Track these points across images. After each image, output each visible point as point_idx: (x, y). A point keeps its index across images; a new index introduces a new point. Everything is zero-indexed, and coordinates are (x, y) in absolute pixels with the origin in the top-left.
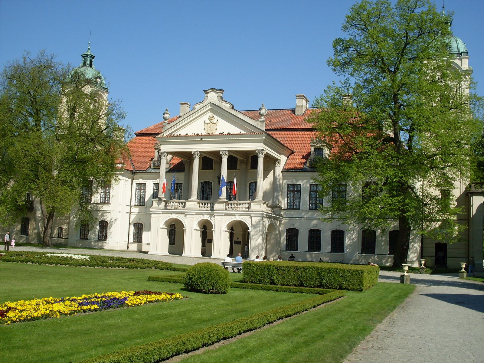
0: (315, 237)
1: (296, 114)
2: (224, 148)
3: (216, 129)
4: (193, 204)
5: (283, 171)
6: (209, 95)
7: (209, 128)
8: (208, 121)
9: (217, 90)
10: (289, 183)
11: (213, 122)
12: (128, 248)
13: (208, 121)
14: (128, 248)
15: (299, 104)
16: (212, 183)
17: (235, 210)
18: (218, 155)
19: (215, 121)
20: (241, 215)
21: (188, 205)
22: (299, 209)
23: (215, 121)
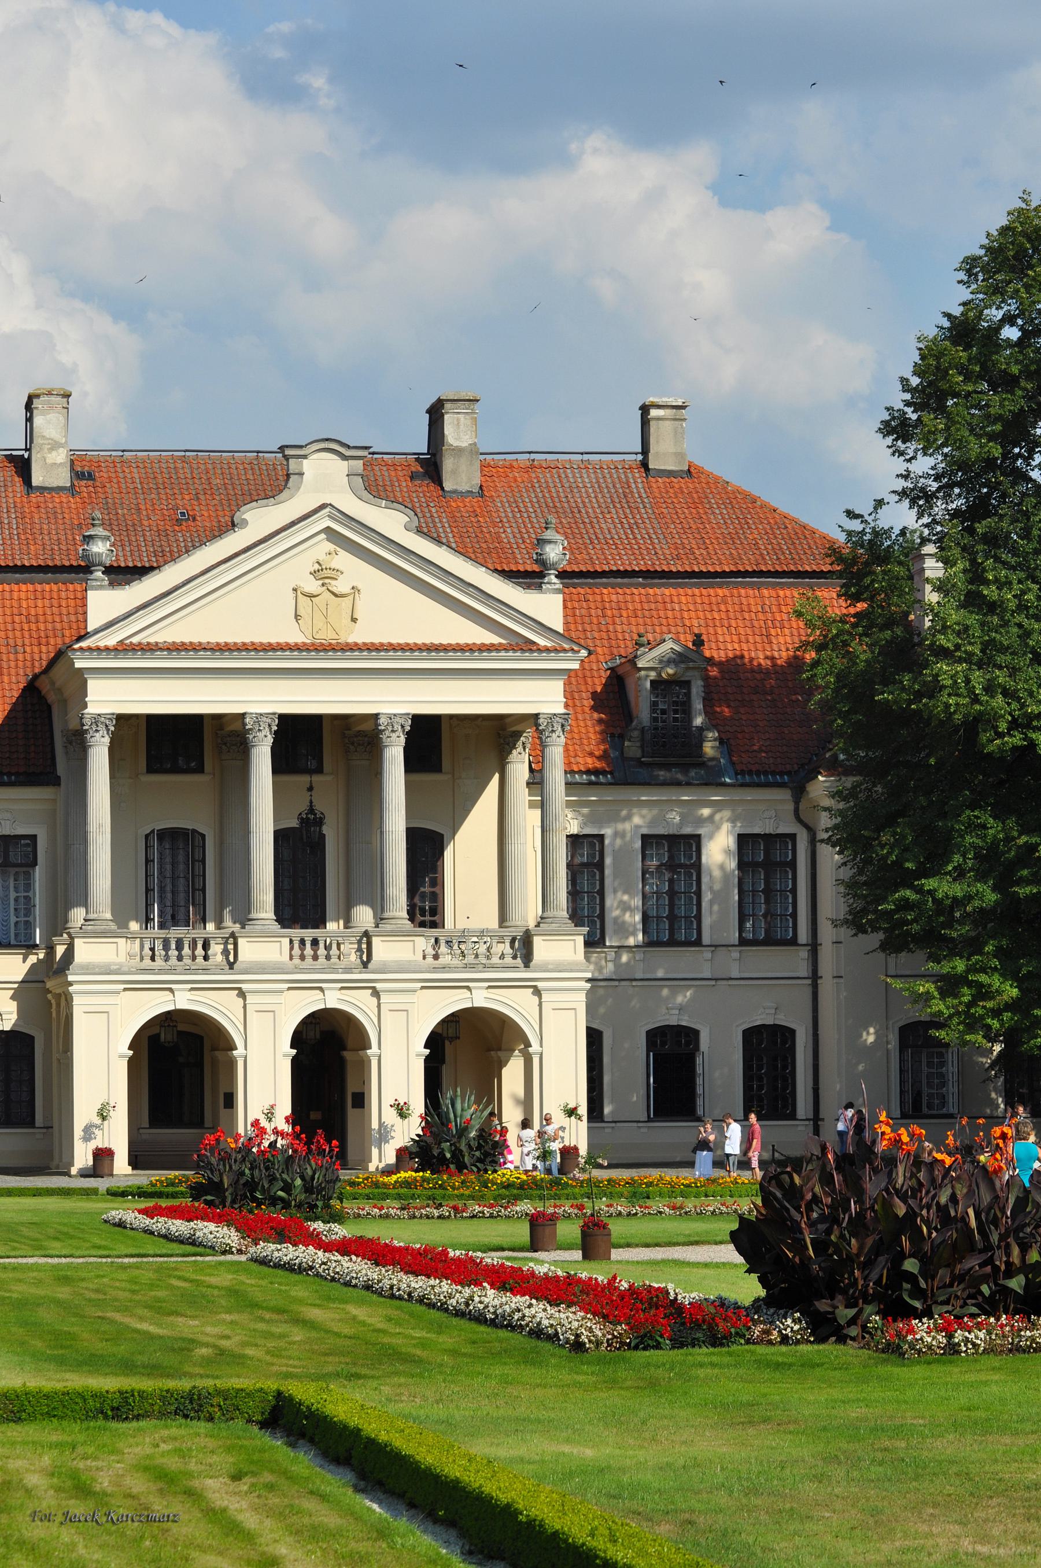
0: (673, 1061)
1: (448, 486)
2: (393, 700)
3: (354, 620)
4: (266, 946)
5: (533, 783)
6: (307, 465)
7: (318, 616)
8: (312, 586)
9: (349, 447)
10: (607, 842)
11: (334, 589)
13: (312, 586)
15: (458, 439)
16: (203, 836)
17: (467, 967)
18: (359, 735)
19: (341, 586)
20: (494, 985)
23: (341, 586)
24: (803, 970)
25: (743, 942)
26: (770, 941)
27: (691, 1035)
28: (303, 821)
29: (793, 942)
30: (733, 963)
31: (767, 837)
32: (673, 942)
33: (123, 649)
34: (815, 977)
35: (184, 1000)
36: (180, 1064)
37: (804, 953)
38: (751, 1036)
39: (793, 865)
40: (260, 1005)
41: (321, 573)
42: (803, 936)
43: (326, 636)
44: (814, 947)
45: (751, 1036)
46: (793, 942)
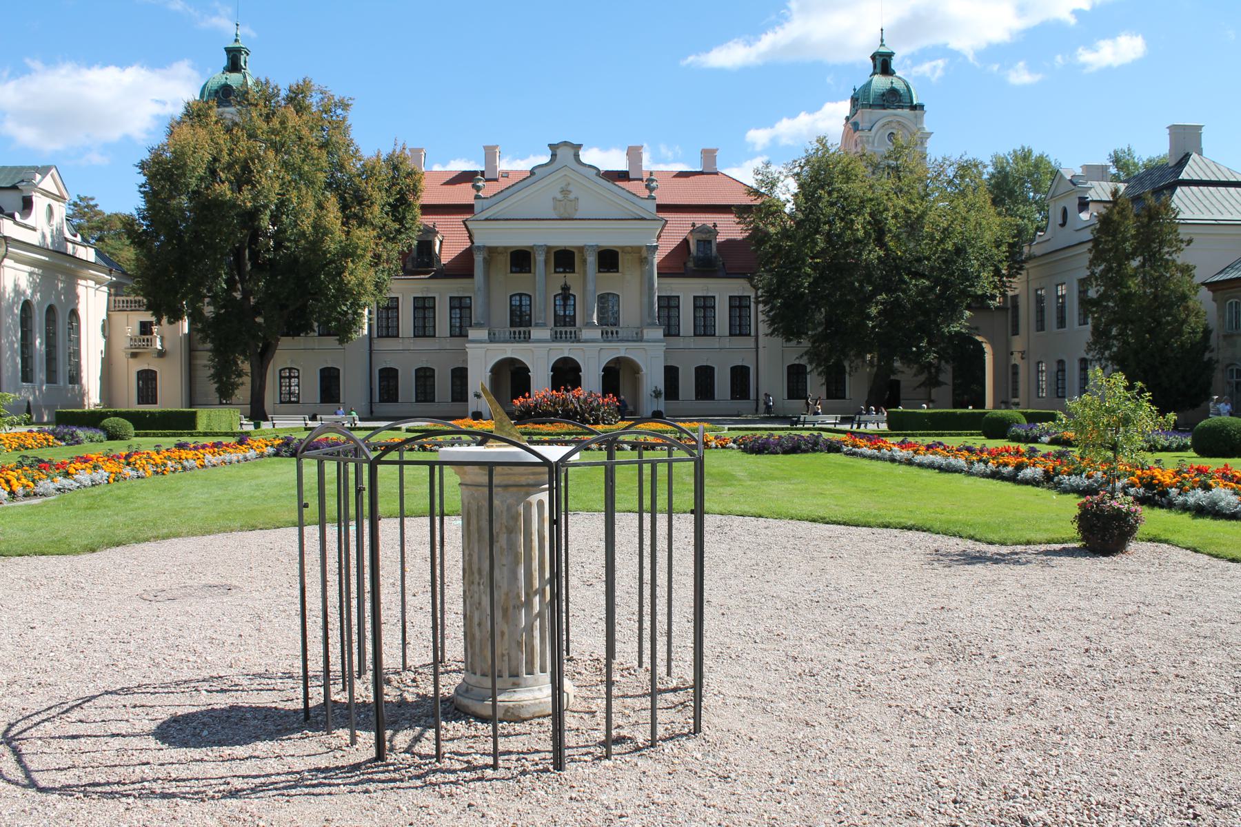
0: (705, 376)
8: (560, 196)
12: (372, 412)
13: (560, 196)
14: (372, 412)
19: (572, 196)
21: (536, 333)
22: (678, 335)
23: (572, 196)
24: (753, 345)
25: (731, 335)
26: (741, 335)
27: (712, 369)
28: (563, 289)
29: (749, 335)
30: (728, 342)
31: (740, 297)
32: (705, 335)
33: (486, 220)
34: (757, 348)
35: (509, 355)
36: (512, 377)
37: (753, 339)
38: (734, 369)
39: (749, 307)
40: (539, 357)
41: (565, 192)
42: (753, 333)
43: (566, 216)
44: (757, 336)
45: (734, 369)
46: (749, 335)
